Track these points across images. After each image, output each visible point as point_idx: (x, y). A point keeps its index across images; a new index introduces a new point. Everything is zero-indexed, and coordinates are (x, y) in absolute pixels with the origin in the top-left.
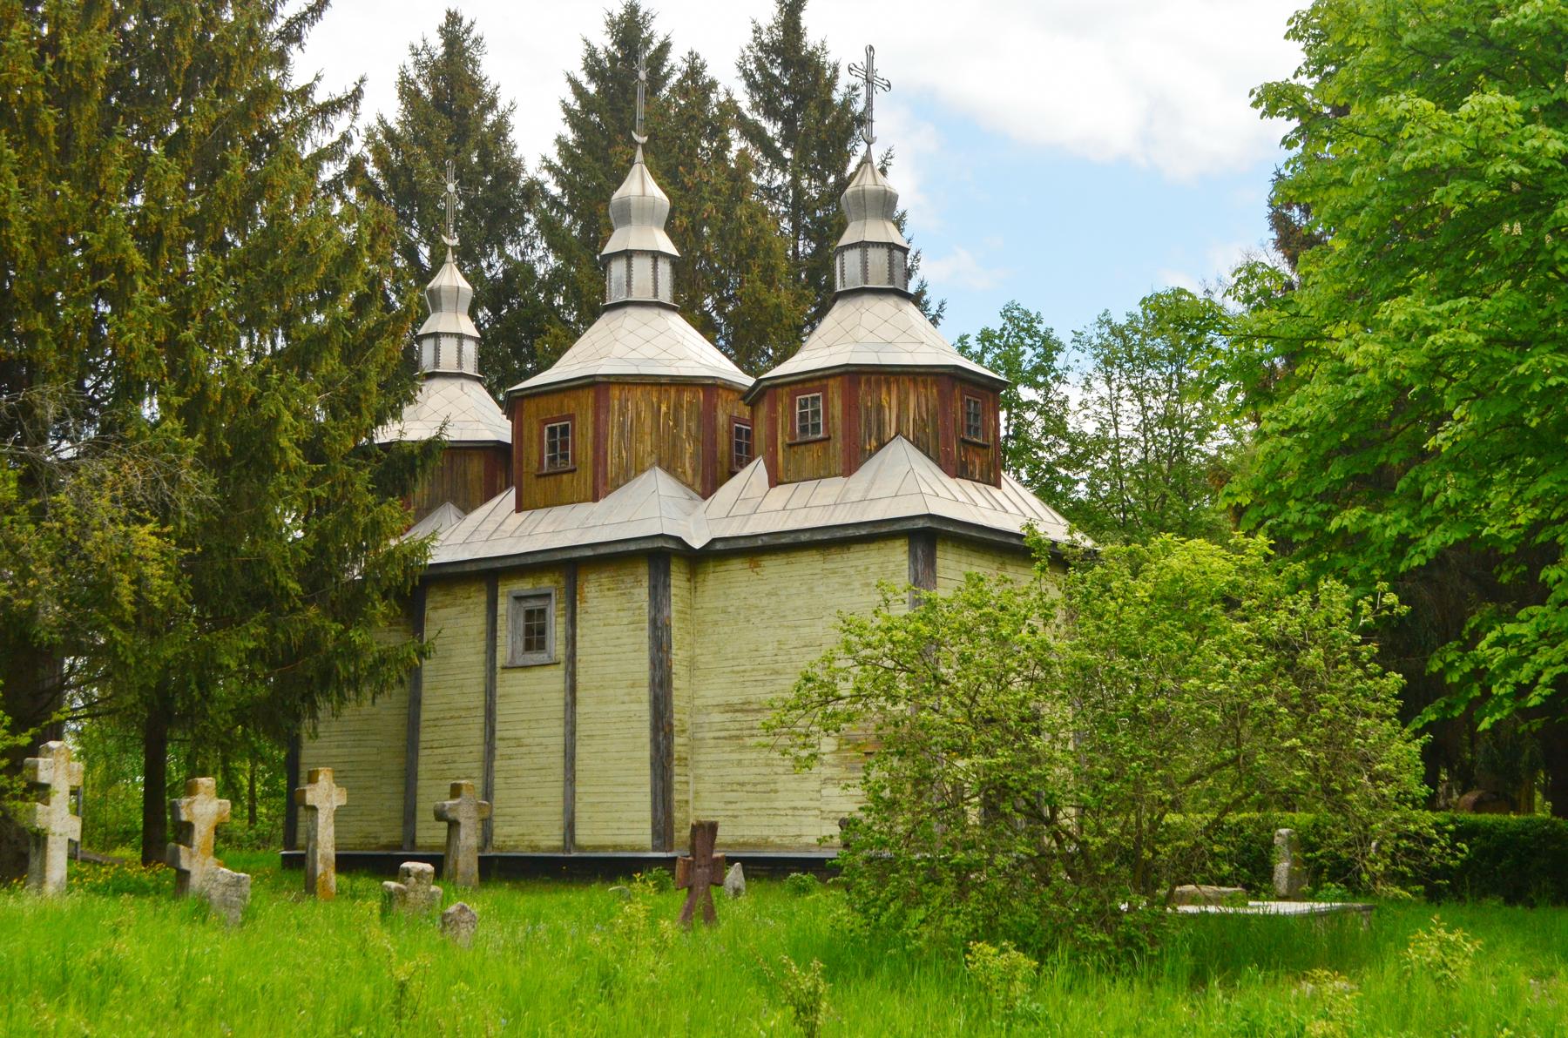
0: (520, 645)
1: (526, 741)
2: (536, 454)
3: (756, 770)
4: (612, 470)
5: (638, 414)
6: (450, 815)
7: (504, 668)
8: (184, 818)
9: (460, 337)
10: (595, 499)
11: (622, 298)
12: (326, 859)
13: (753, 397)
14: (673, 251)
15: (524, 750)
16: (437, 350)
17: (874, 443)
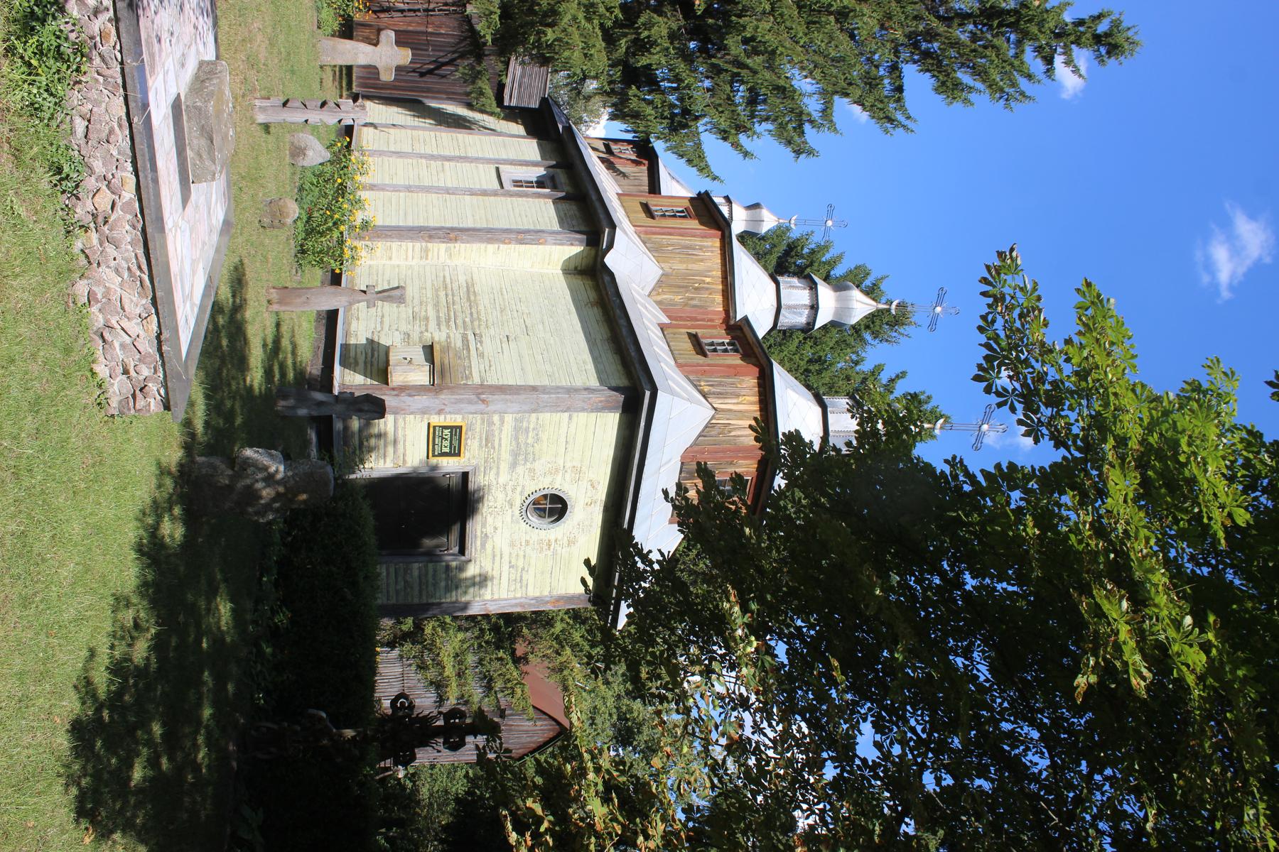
1: (441, 175)
3: (416, 296)
5: (702, 261)
7: (497, 169)
17: (706, 389)
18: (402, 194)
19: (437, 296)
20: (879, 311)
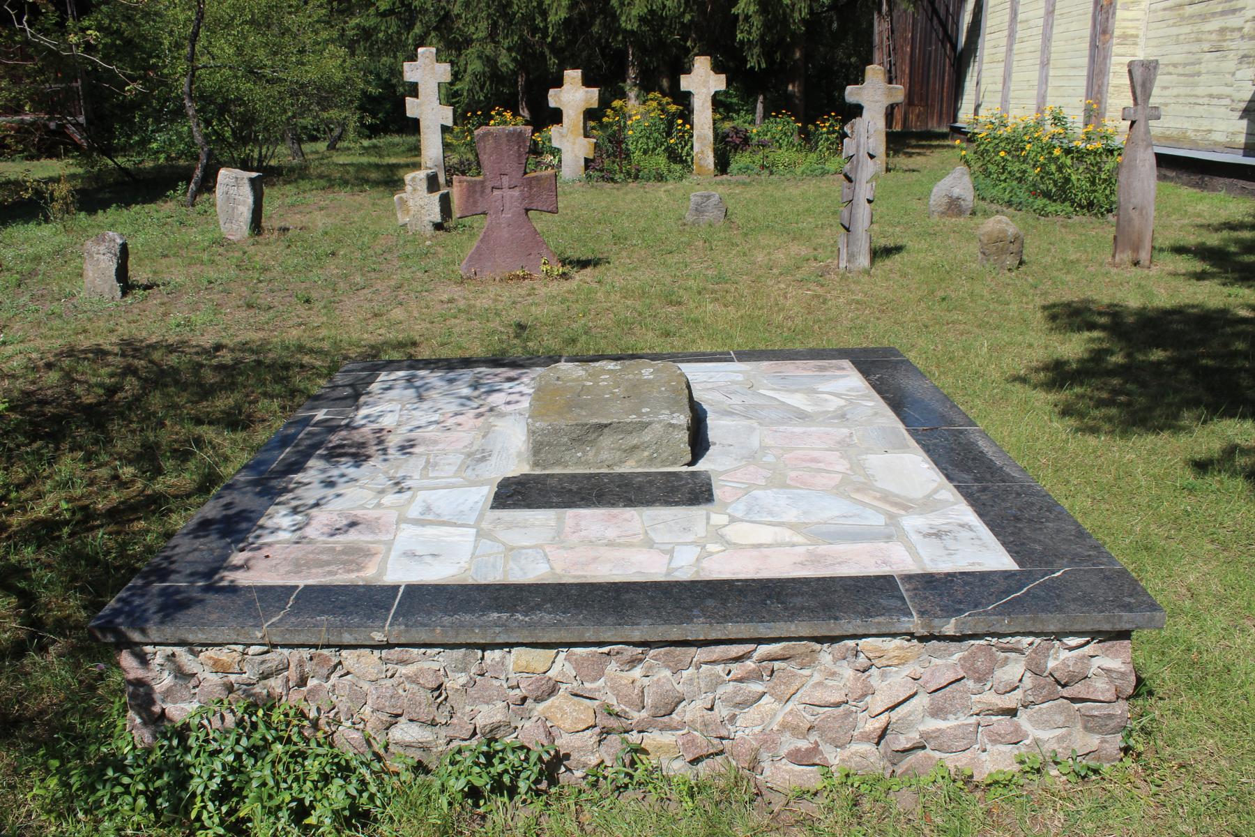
1: (1032, 23)
3: (1186, 48)
15: (1029, 32)
18: (1051, 73)
19: (1191, 17)
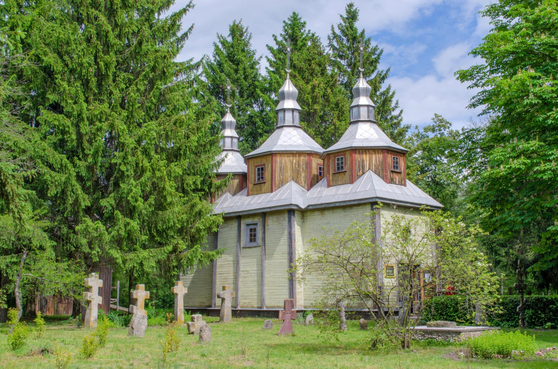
0: (249, 240)
1: (250, 272)
2: (253, 178)
4: (277, 182)
5: (286, 163)
6: (222, 296)
8: (135, 297)
9: (232, 137)
10: (272, 192)
11: (282, 125)
12: (180, 310)
13: (327, 156)
14: (300, 108)
15: (250, 275)
16: (224, 142)
17: (361, 172)
20: (290, 78)
